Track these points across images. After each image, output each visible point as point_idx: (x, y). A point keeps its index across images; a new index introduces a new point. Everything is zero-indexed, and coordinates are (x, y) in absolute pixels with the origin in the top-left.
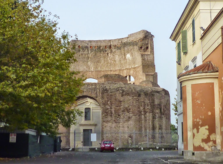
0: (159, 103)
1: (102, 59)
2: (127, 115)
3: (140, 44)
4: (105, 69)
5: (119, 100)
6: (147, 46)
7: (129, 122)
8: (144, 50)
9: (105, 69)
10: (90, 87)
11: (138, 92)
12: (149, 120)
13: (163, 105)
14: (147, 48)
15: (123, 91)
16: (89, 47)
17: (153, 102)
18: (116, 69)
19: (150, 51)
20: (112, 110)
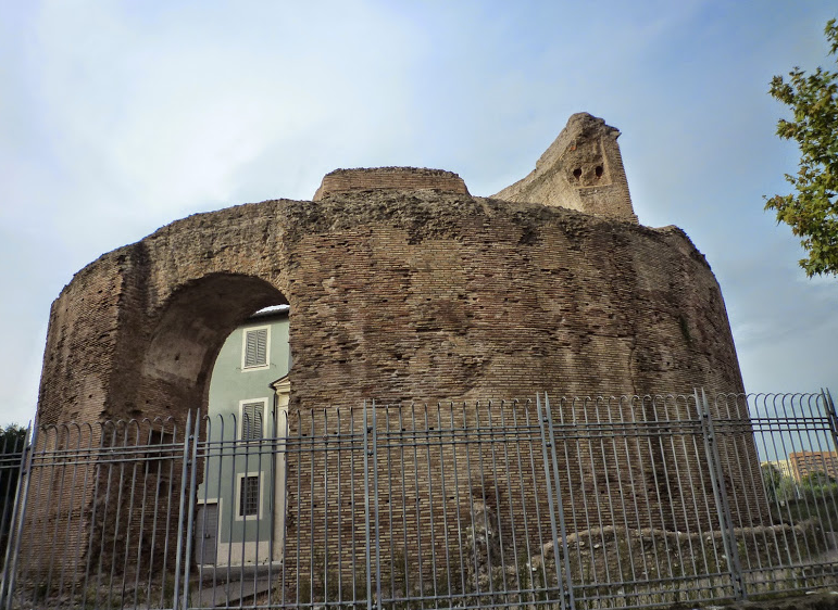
0: (666, 289)
2: (455, 350)
3: (569, 166)
5: (392, 264)
6: (599, 163)
7: (473, 391)
8: (589, 176)
10: (244, 225)
11: (516, 220)
12: (615, 378)
13: (689, 303)
14: (599, 171)
15: (422, 217)
17: (630, 276)
19: (612, 176)
20: (347, 325)
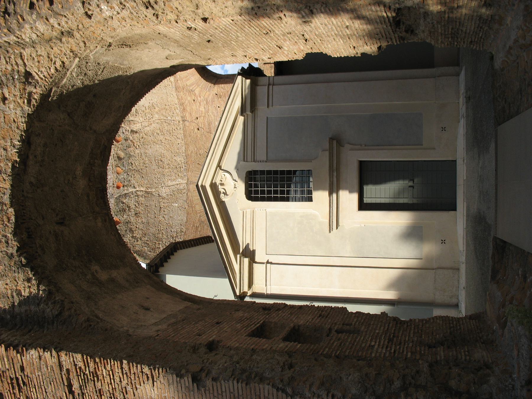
1: (150, 152)
4: (179, 141)
9: (179, 141)
16: (118, 191)
18: (177, 102)
